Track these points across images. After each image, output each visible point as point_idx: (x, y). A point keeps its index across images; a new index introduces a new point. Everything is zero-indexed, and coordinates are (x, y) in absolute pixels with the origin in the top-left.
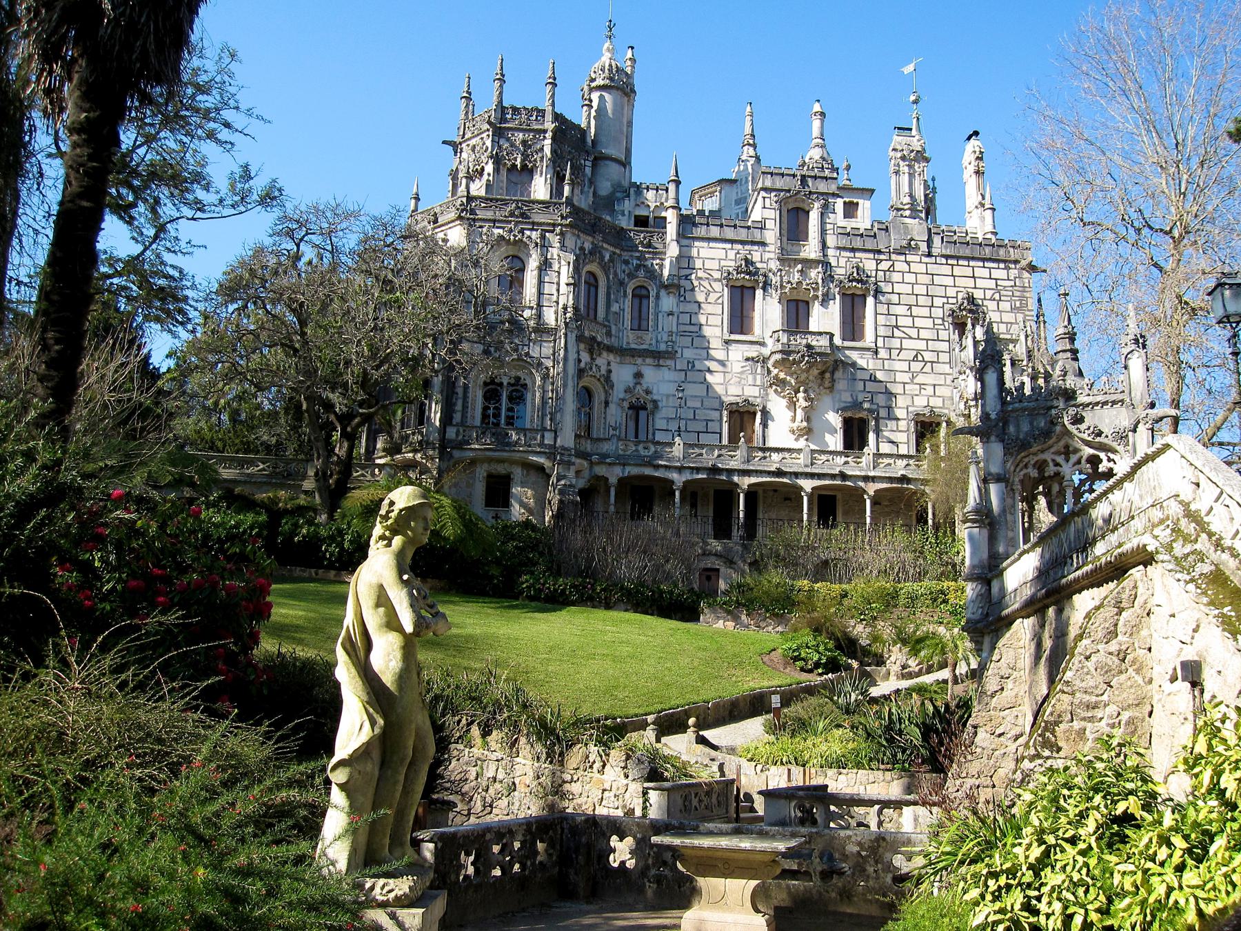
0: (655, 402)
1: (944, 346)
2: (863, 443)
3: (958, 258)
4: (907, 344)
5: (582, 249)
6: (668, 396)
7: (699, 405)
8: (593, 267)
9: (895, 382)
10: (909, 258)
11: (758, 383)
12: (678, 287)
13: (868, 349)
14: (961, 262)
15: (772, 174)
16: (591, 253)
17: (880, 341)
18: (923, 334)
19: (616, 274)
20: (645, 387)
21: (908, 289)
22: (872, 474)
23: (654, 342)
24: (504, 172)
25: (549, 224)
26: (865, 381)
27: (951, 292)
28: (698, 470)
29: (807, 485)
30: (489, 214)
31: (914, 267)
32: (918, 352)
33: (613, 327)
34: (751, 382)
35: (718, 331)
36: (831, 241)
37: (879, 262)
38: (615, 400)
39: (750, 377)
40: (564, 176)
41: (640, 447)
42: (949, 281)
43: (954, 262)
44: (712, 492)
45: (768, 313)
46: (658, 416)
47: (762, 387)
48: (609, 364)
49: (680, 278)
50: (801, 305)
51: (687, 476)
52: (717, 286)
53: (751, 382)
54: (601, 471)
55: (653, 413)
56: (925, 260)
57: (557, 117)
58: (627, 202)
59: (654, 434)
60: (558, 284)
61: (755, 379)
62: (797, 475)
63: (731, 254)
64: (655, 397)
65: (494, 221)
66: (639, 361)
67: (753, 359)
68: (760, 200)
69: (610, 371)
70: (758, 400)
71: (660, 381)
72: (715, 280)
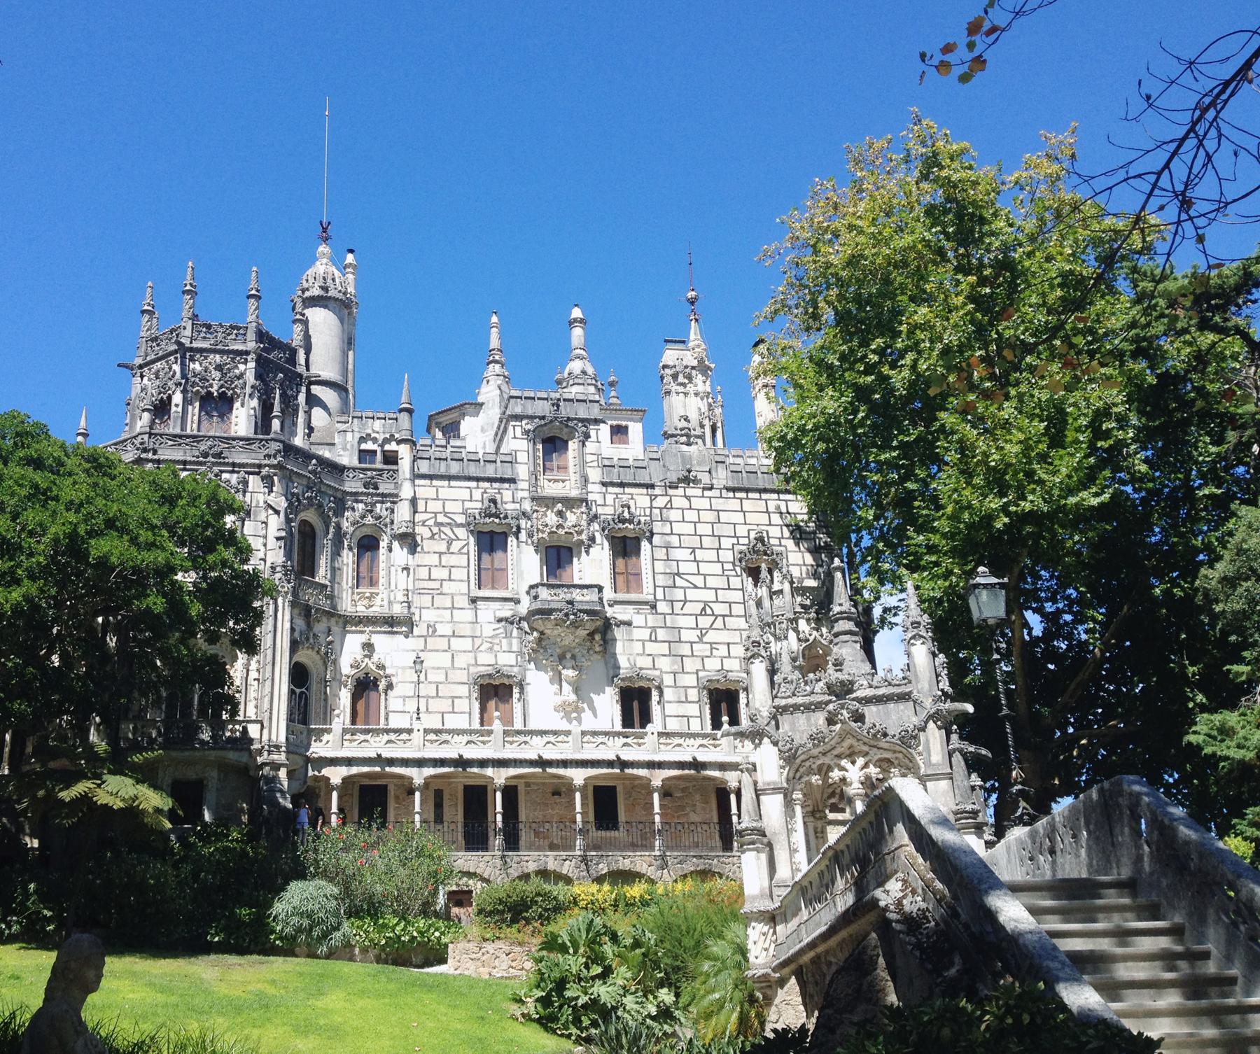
1: (737, 596)
2: (646, 718)
3: (747, 490)
4: (691, 594)
6: (403, 668)
7: (442, 678)
8: (310, 516)
9: (680, 641)
10: (689, 492)
11: (515, 648)
13: (646, 603)
14: (750, 495)
17: (660, 592)
18: (712, 582)
21: (689, 529)
22: (657, 758)
23: (385, 603)
25: (253, 465)
26: (643, 641)
27: (742, 531)
28: (441, 762)
29: (578, 776)
30: (178, 455)
31: (696, 503)
32: (706, 603)
34: (505, 648)
35: (463, 588)
36: (595, 475)
37: (653, 498)
39: (504, 641)
40: (272, 405)
42: (738, 518)
43: (743, 495)
44: (461, 788)
45: (523, 563)
47: (520, 653)
50: (563, 551)
51: (429, 771)
52: (462, 533)
53: (505, 648)
56: (707, 493)
57: (261, 336)
58: (349, 435)
59: (387, 719)
60: (265, 537)
61: (510, 645)
62: (565, 764)
63: (477, 494)
64: (388, 671)
65: (185, 463)
67: (506, 620)
68: (511, 428)
70: (516, 669)
71: (393, 652)
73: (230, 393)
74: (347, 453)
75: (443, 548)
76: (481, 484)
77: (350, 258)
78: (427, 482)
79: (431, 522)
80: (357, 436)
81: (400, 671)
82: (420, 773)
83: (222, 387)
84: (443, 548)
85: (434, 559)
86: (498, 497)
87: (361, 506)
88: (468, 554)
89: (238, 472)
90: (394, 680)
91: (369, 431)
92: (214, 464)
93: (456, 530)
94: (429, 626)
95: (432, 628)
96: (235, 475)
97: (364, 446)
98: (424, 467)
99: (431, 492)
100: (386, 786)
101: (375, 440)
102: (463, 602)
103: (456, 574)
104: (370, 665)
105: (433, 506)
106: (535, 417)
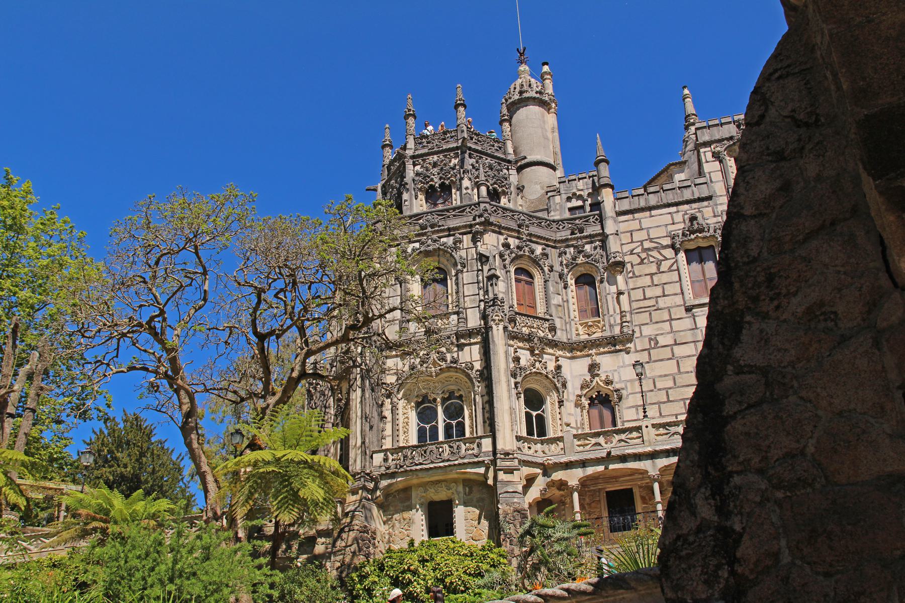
0: (616, 391)
5: (506, 246)
6: (631, 381)
8: (524, 264)
12: (622, 264)
15: (709, 127)
16: (519, 248)
19: (551, 269)
20: (603, 378)
24: (421, 197)
25: (465, 227)
33: (558, 323)
35: (678, 300)
38: (573, 398)
41: (601, 440)
46: (624, 406)
48: (557, 360)
49: (624, 255)
52: (669, 253)
54: (558, 476)
55: (617, 403)
63: (678, 218)
64: (618, 386)
66: (593, 351)
69: (559, 368)
72: (667, 247)
73: (447, 182)
74: (558, 213)
75: (653, 269)
76: (681, 208)
77: (546, 68)
78: (630, 217)
79: (639, 250)
80: (564, 197)
81: (629, 384)
82: (654, 465)
83: (441, 178)
84: (653, 269)
85: (647, 281)
86: (698, 214)
87: (572, 249)
88: (678, 270)
89: (454, 235)
90: (624, 393)
91: (574, 191)
92: (433, 233)
93: (663, 252)
94: (650, 340)
95: (653, 340)
96: (452, 238)
97: (570, 205)
98: (625, 205)
99: (635, 225)
100: (631, 489)
101: (580, 197)
102: (681, 312)
103: (669, 289)
104: (601, 383)
105: (637, 236)
106: (723, 140)
